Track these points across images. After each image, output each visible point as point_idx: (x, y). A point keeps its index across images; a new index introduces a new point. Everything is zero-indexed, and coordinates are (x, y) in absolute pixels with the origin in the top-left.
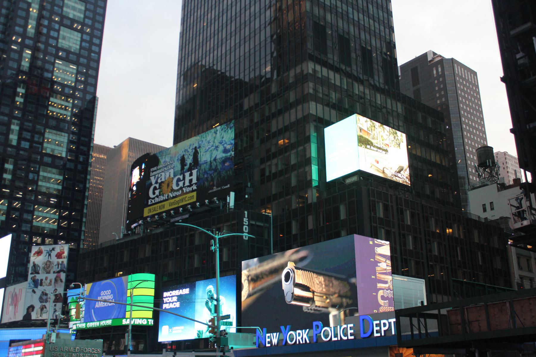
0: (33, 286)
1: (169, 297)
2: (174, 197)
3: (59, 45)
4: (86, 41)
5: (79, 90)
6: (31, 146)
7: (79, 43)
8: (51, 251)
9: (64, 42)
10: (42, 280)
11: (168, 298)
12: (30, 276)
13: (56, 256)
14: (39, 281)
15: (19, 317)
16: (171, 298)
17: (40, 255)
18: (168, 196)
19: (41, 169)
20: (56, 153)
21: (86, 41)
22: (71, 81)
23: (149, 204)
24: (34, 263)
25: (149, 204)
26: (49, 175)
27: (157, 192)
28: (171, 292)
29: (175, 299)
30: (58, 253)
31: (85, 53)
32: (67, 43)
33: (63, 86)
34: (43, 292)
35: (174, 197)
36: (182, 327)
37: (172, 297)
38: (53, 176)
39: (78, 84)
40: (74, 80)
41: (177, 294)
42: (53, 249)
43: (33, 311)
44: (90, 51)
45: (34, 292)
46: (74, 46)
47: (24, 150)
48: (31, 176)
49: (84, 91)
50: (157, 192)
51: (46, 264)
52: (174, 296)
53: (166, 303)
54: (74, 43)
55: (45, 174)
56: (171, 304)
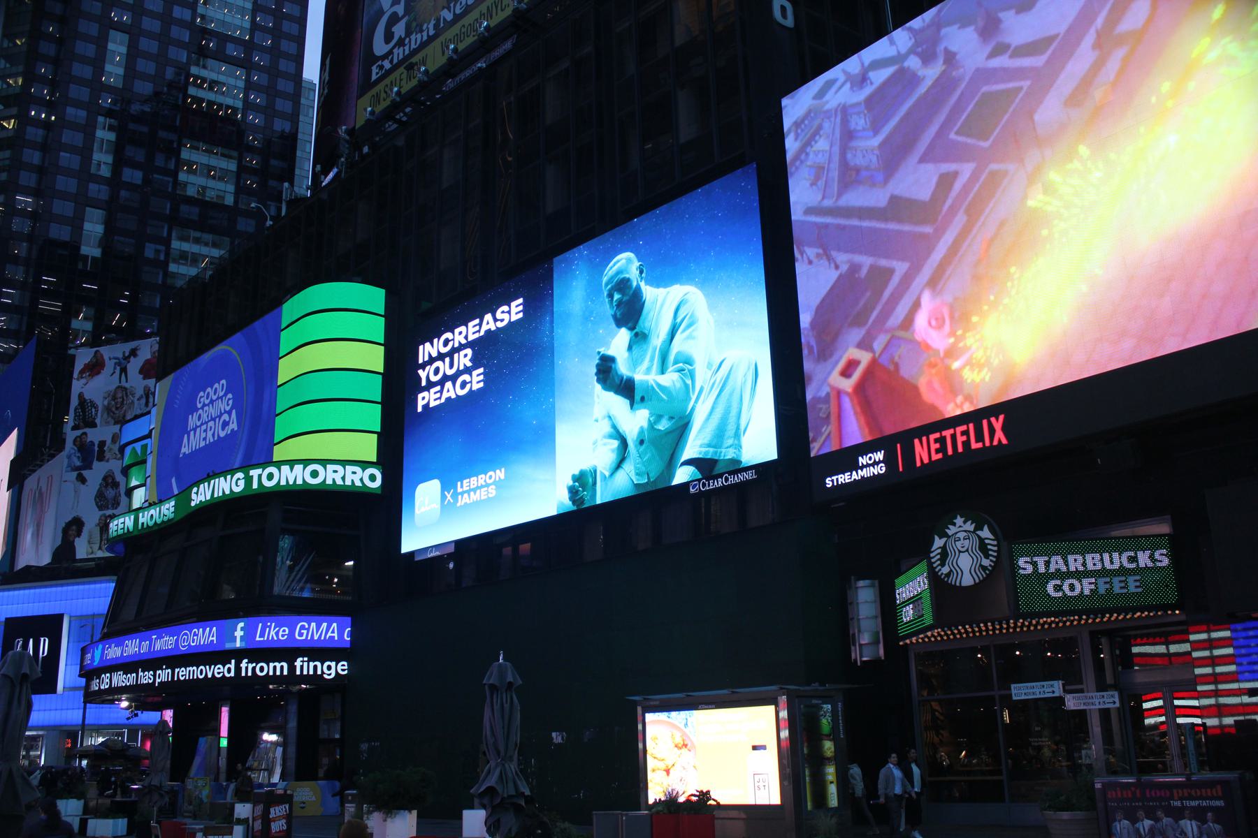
0: (78, 463)
1: (441, 357)
2: (457, 18)
5: (263, 49)
6: (146, 181)
8: (127, 358)
10: (102, 444)
11: (439, 364)
12: (71, 436)
13: (140, 372)
14: (96, 448)
15: (45, 559)
16: (449, 366)
17: (98, 373)
18: (436, 26)
19: (174, 234)
20: (210, 195)
22: (241, 28)
23: (374, 77)
24: (81, 396)
25: (374, 77)
26: (196, 249)
27: (399, 30)
28: (448, 335)
29: (464, 359)
30: (147, 362)
33: (224, 39)
34: (105, 479)
35: (457, 18)
36: (500, 474)
37: (451, 354)
38: (204, 250)
39: (257, 33)
40: (247, 25)
41: (471, 338)
42: (134, 353)
43: (79, 534)
45: (82, 479)
47: (131, 187)
48: (150, 251)
49: (274, 52)
50: (399, 30)
51: (114, 398)
52: (462, 347)
53: (430, 385)
55: (186, 246)
56: (449, 385)
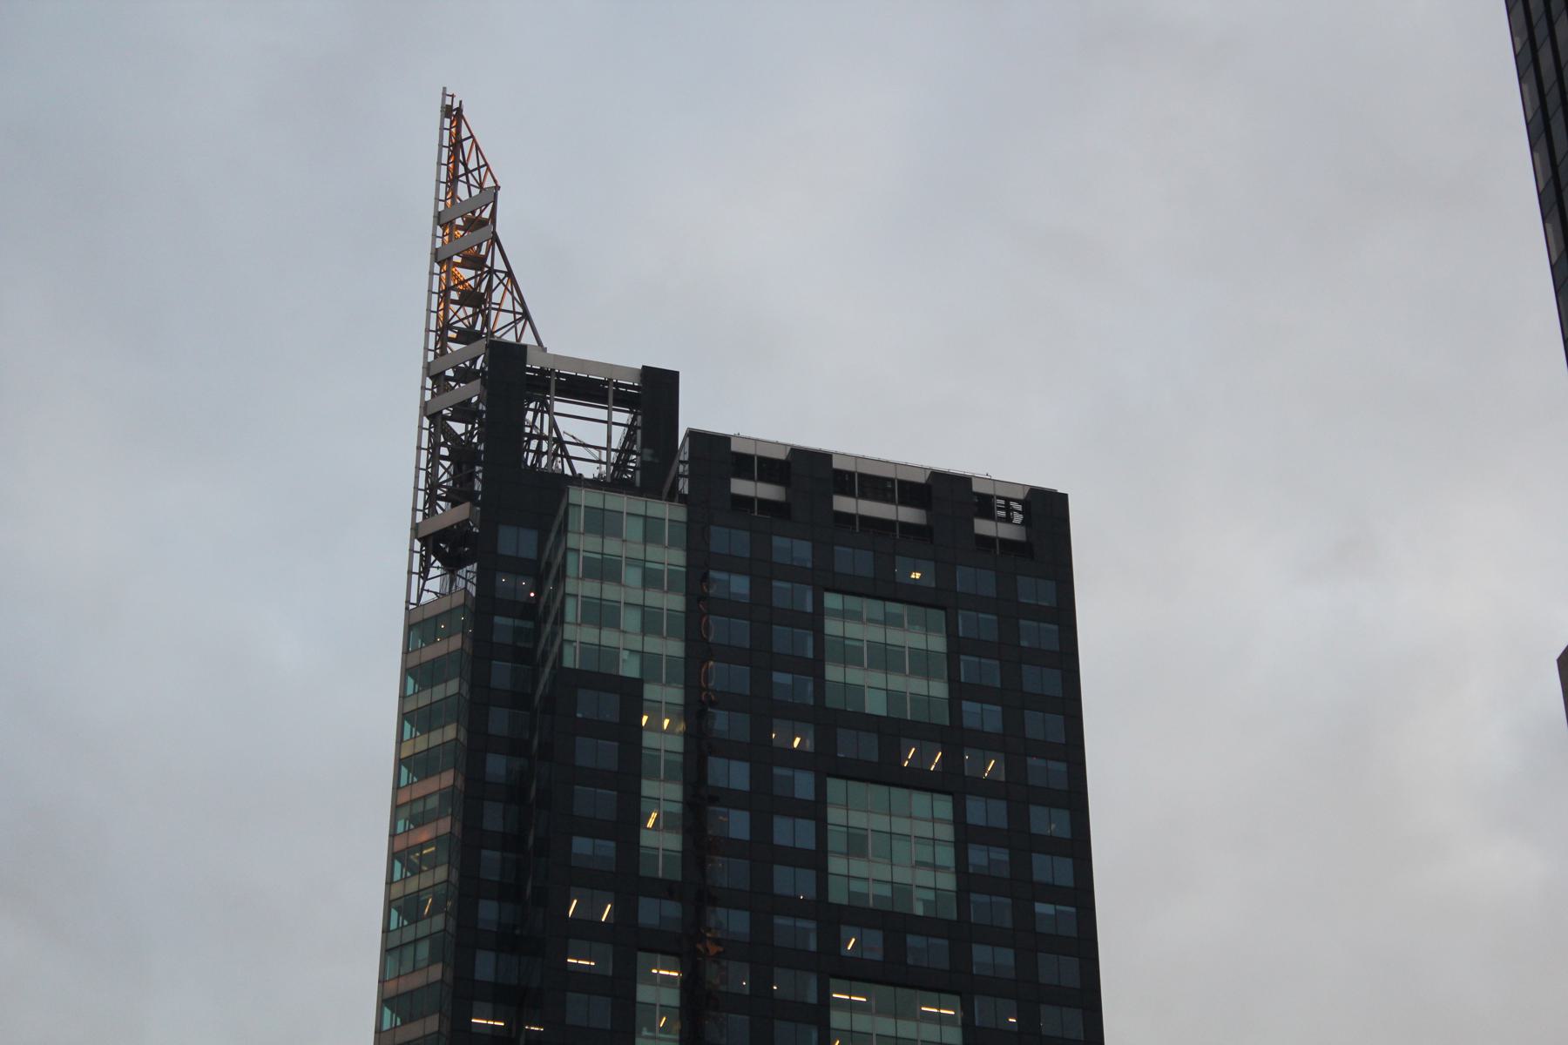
3: (837, 895)
4: (986, 836)
7: (946, 856)
9: (859, 867)
21: (986, 836)
31: (993, 909)
32: (882, 871)
44: (1022, 889)
46: (925, 877)
54: (920, 864)
